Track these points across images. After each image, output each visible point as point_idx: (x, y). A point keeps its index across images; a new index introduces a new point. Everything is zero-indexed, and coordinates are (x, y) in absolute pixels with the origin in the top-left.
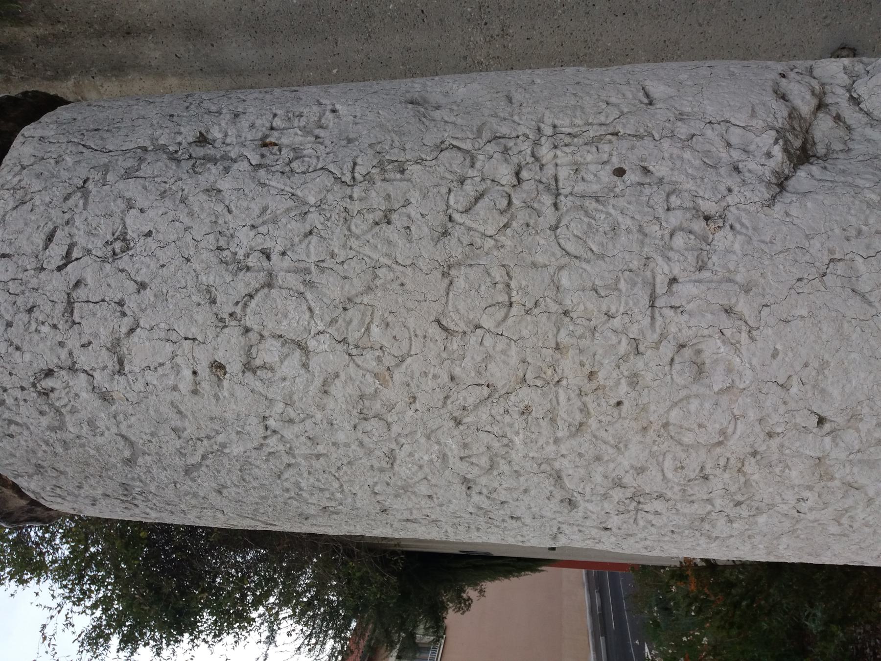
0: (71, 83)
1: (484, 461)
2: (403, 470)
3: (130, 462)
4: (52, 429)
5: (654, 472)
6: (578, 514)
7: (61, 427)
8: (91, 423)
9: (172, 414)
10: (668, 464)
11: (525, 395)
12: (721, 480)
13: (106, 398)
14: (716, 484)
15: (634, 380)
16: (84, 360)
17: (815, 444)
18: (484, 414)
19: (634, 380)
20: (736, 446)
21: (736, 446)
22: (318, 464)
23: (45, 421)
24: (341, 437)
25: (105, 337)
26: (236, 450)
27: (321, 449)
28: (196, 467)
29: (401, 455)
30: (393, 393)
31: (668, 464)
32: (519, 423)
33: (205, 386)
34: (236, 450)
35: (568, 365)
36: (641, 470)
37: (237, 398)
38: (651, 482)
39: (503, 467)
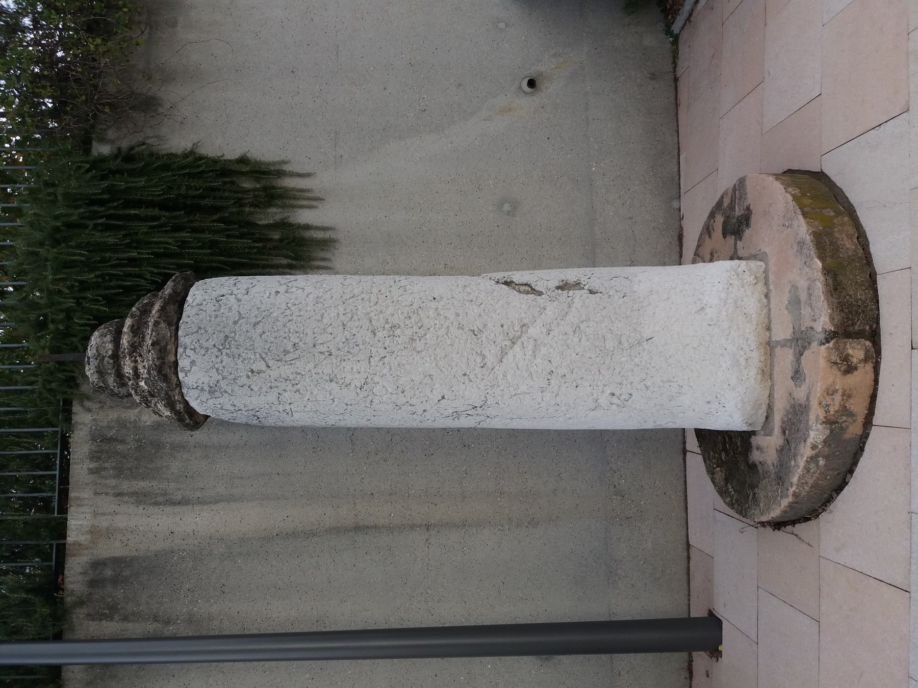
0: (137, 411)
1: (350, 315)
2: (325, 321)
3: (235, 323)
4: (215, 311)
5: (396, 315)
6: (376, 338)
7: (219, 310)
8: (230, 309)
9: (259, 303)
10: (400, 312)
11: (363, 296)
12: (414, 318)
13: (239, 300)
14: (413, 320)
15: (390, 291)
16: (236, 292)
17: (434, 304)
18: (351, 300)
19: (390, 291)
20: (415, 306)
21: (415, 306)
22: (299, 319)
23: (214, 308)
24: (309, 308)
25: (245, 287)
26: (275, 314)
27: (302, 313)
28: (258, 322)
29: (325, 315)
30: (327, 296)
31: (400, 312)
32: (360, 302)
33: (272, 296)
34: (275, 314)
35: (375, 290)
36: (393, 315)
37: (282, 298)
38: (395, 320)
39: (355, 317)
